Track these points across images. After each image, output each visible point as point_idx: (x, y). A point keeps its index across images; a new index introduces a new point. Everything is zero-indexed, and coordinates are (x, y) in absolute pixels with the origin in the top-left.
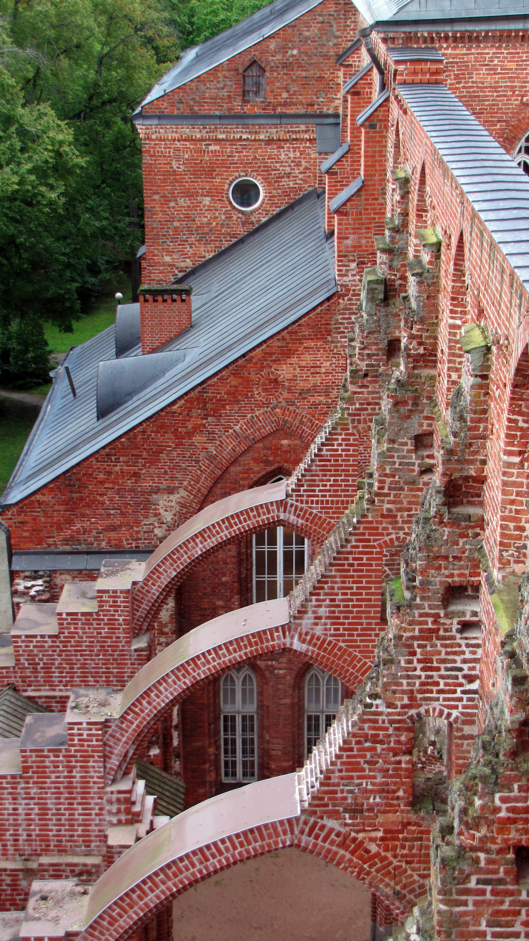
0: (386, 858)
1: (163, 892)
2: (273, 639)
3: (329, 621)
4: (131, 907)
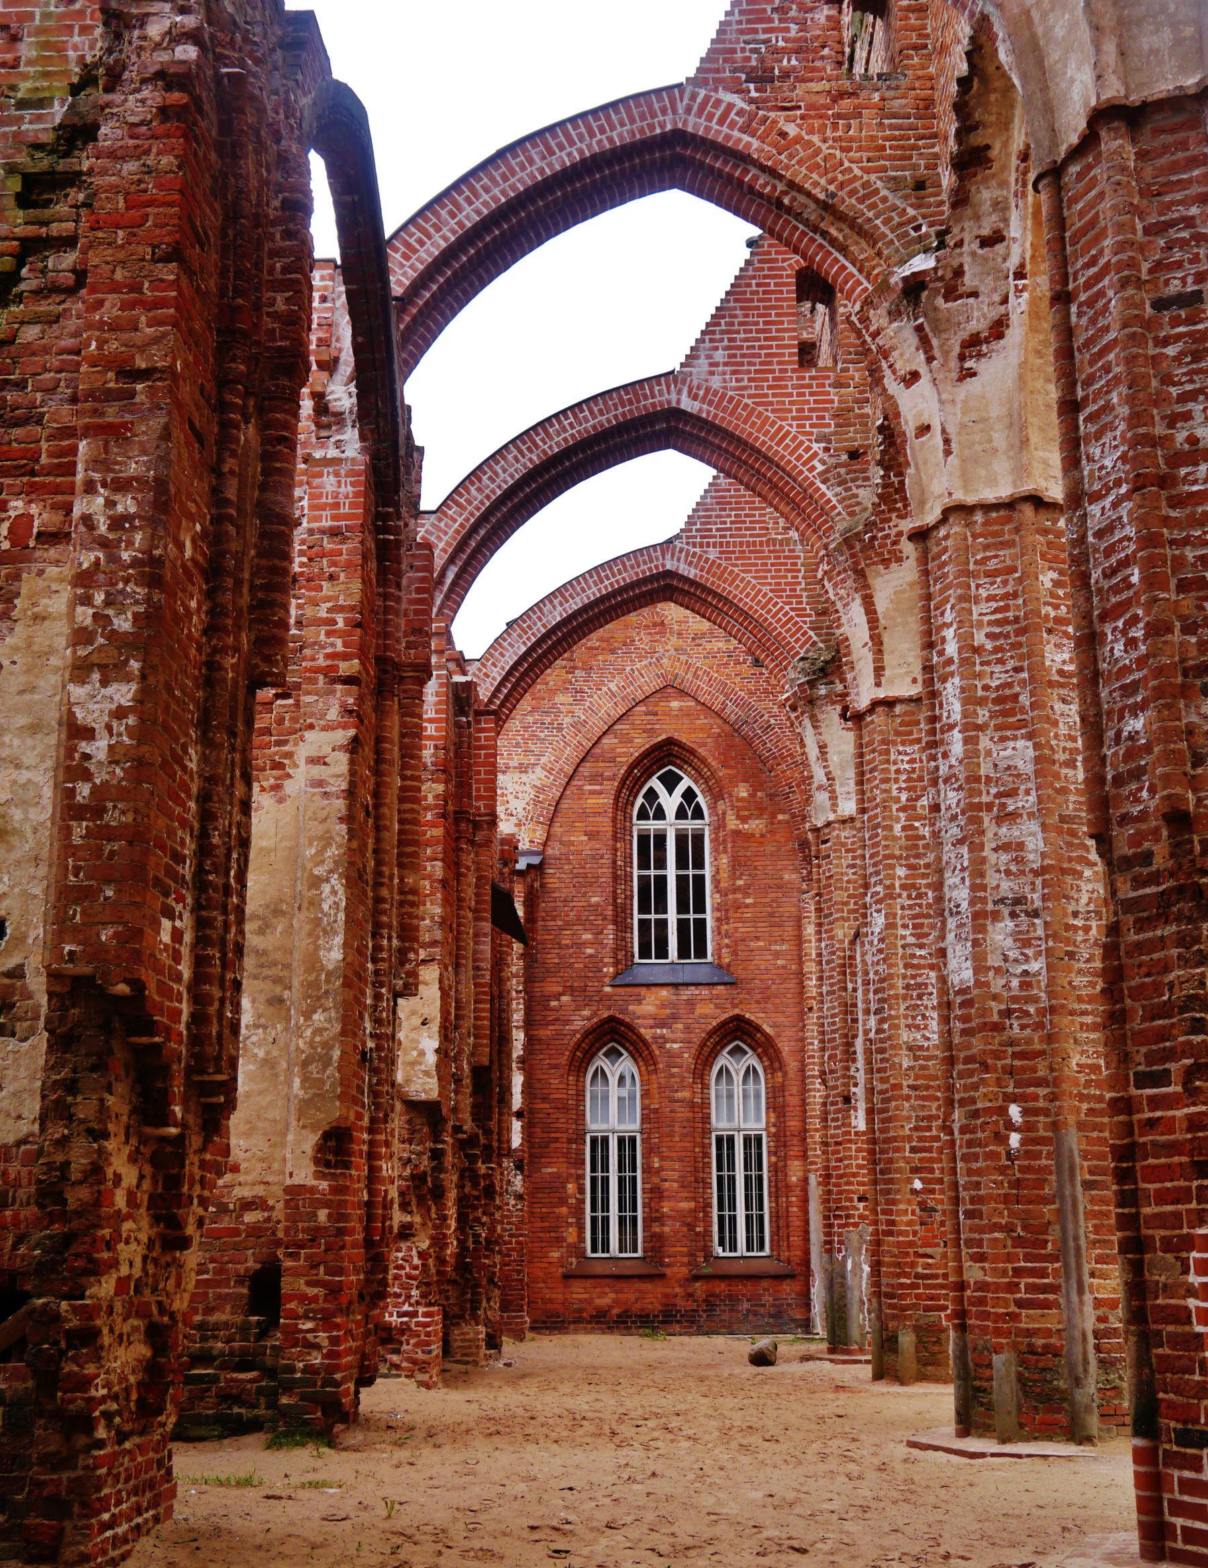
0: (810, 144)
1: (485, 204)
2: (653, 396)
3: (728, 369)
4: (438, 230)
